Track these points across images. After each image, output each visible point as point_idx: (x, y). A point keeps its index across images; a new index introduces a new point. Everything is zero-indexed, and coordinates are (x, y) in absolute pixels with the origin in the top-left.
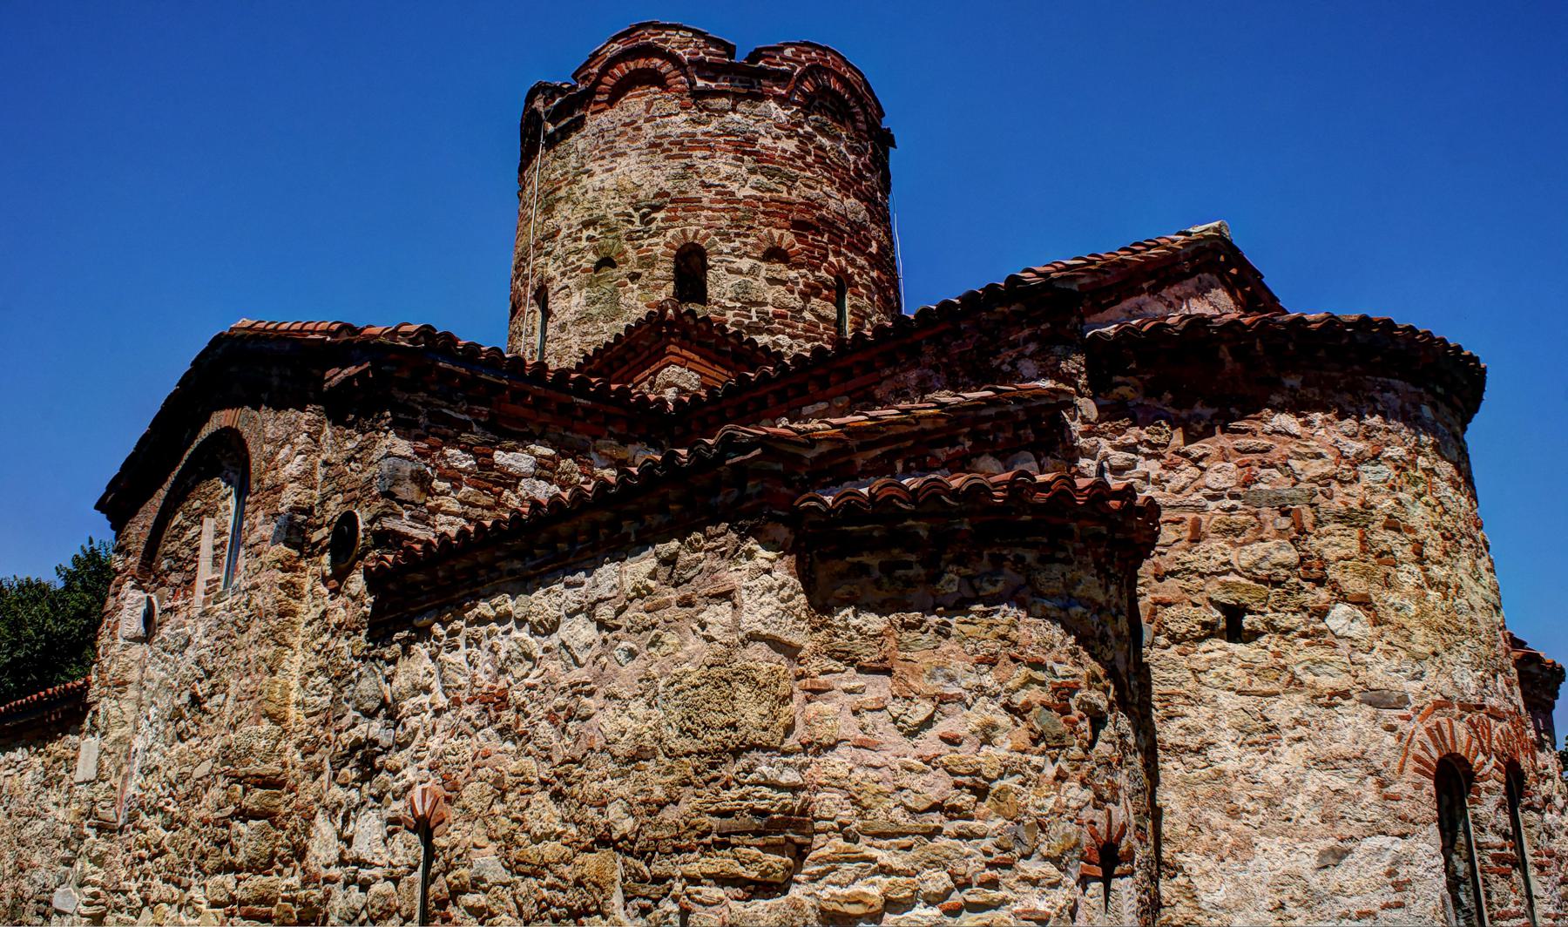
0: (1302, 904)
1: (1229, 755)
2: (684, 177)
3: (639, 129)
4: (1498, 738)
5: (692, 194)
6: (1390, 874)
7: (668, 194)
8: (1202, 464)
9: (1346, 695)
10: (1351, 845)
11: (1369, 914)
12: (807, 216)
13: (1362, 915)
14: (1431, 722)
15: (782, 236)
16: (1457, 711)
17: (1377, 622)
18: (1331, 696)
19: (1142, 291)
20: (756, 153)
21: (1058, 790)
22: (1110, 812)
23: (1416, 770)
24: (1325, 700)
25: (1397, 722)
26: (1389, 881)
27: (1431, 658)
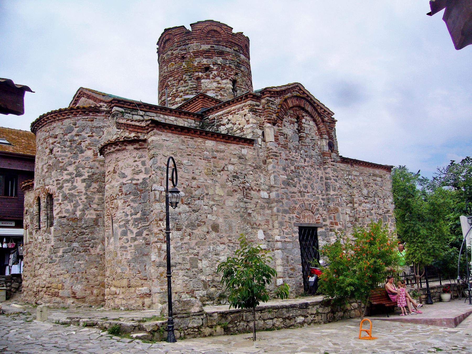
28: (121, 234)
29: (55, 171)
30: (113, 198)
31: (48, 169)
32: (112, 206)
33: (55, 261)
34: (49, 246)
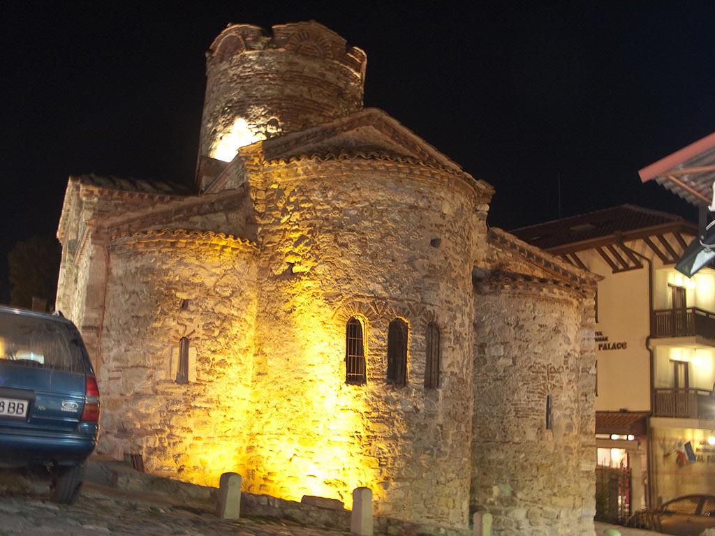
28: (567, 428)
29: (444, 282)
31: (429, 271)
32: (553, 382)
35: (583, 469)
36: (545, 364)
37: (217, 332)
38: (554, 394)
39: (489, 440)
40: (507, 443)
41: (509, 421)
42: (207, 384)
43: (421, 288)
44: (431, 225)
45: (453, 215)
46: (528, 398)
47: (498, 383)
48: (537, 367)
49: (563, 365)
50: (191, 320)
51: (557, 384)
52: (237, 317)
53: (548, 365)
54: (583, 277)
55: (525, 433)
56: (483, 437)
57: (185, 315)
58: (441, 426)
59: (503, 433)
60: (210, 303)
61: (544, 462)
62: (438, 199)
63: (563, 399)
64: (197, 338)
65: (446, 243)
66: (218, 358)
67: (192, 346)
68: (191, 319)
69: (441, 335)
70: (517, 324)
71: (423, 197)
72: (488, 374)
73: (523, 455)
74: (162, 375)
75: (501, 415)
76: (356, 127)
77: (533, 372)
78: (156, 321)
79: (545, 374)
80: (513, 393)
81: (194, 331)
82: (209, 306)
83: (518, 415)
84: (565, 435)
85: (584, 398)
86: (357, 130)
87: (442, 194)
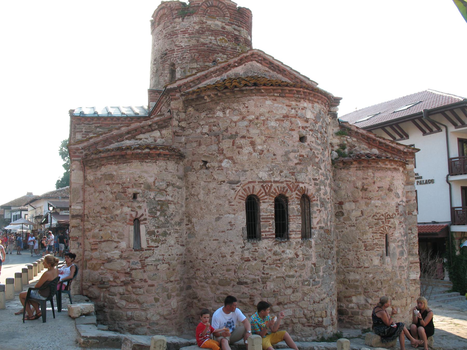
0: (212, 229)
1: (201, 197)
2: (171, 44)
3: (162, 32)
4: (275, 189)
5: (172, 49)
6: (229, 223)
7: (168, 50)
8: (202, 127)
9: (224, 182)
10: (222, 216)
11: (224, 231)
12: (203, 47)
13: (223, 232)
14: (246, 186)
15: (195, 55)
16: (257, 183)
17: (234, 163)
18: (221, 182)
19: (212, 77)
20: (188, 33)
21: (122, 209)
22: (137, 212)
23: (239, 199)
24: (220, 183)
25: (235, 187)
26: (229, 224)
27: (250, 171)
28: (399, 254)
29: (311, 166)
30: (389, 216)
31: (300, 160)
32: (389, 225)
33: (319, 282)
34: (309, 264)
35: (411, 278)
36: (384, 213)
37: (158, 213)
38: (390, 232)
39: (348, 266)
40: (360, 267)
41: (361, 253)
42: (155, 248)
43: (295, 172)
44: (299, 128)
45: (314, 119)
46: (373, 237)
47: (353, 228)
48: (378, 216)
49: (395, 212)
50: (140, 207)
51: (392, 226)
52: (172, 201)
53: (385, 214)
54: (405, 150)
55: (372, 260)
56: (344, 265)
57: (135, 204)
58: (314, 264)
59: (357, 261)
60: (152, 195)
61: (385, 278)
62: (302, 109)
63: (396, 235)
64: (145, 219)
65: (310, 138)
66: (161, 231)
67: (142, 224)
68: (140, 206)
69: (311, 203)
70: (363, 187)
71: (292, 109)
72: (345, 222)
73: (371, 276)
74: (123, 245)
75: (355, 249)
76: (244, 63)
77: (375, 219)
78: (117, 209)
79: (384, 220)
80: (363, 234)
81: (143, 215)
82: (152, 197)
83: (367, 249)
84: (399, 259)
85: (410, 231)
86: (245, 65)
87: (305, 105)
